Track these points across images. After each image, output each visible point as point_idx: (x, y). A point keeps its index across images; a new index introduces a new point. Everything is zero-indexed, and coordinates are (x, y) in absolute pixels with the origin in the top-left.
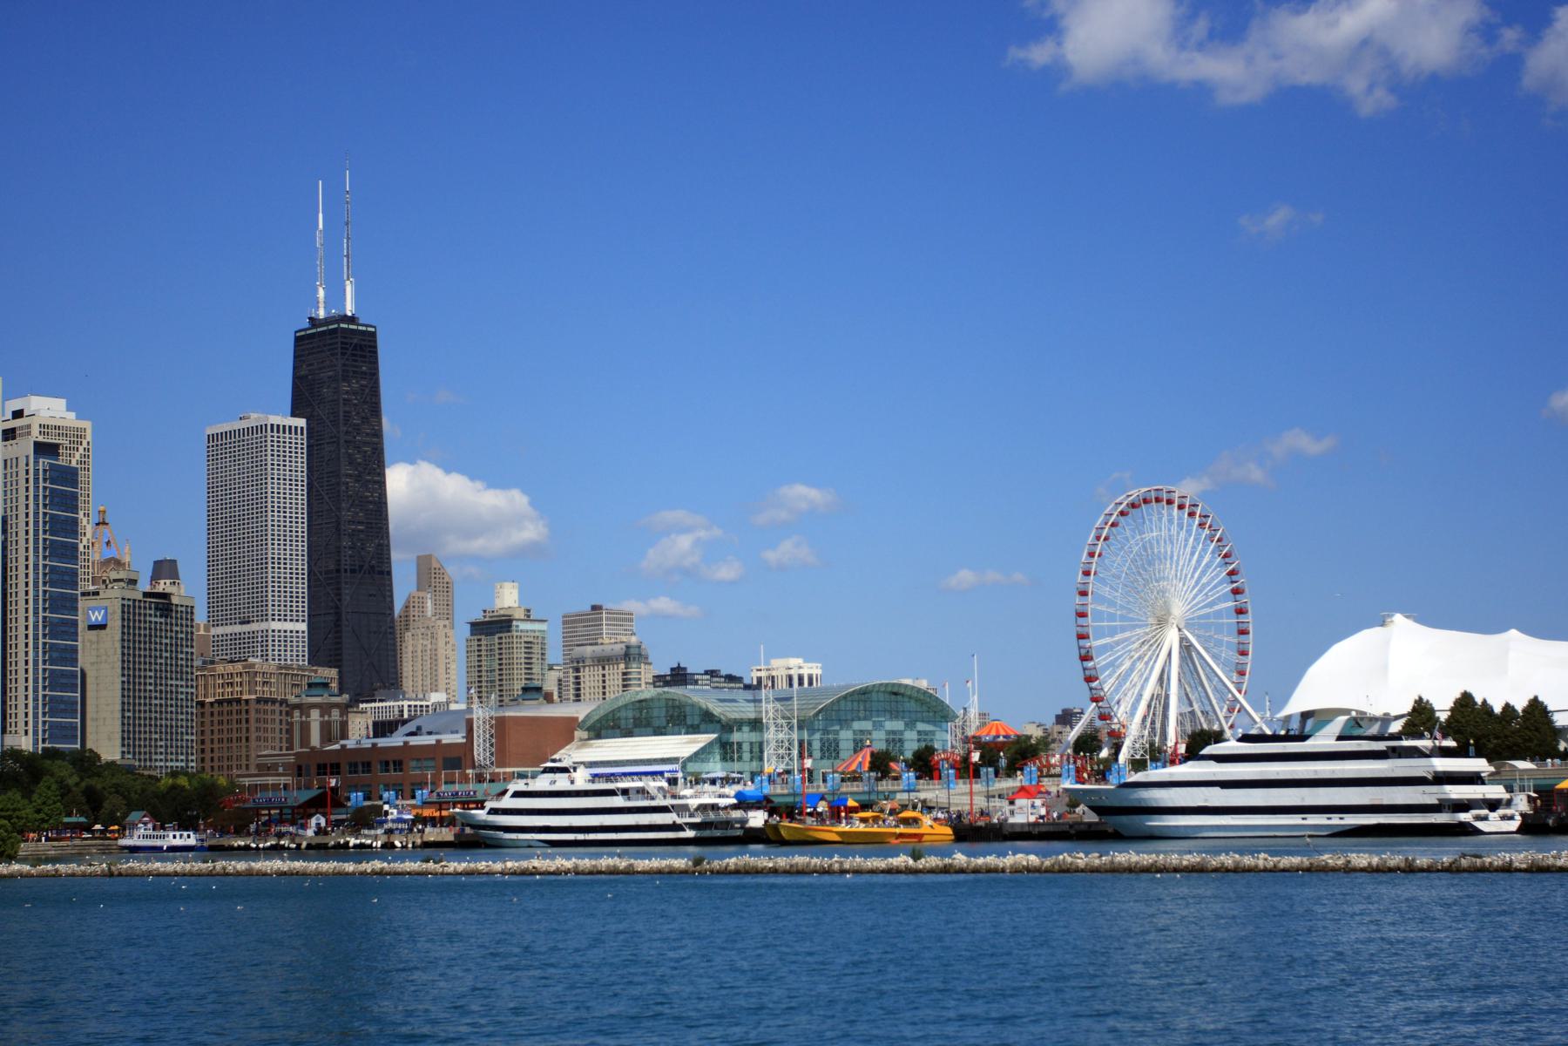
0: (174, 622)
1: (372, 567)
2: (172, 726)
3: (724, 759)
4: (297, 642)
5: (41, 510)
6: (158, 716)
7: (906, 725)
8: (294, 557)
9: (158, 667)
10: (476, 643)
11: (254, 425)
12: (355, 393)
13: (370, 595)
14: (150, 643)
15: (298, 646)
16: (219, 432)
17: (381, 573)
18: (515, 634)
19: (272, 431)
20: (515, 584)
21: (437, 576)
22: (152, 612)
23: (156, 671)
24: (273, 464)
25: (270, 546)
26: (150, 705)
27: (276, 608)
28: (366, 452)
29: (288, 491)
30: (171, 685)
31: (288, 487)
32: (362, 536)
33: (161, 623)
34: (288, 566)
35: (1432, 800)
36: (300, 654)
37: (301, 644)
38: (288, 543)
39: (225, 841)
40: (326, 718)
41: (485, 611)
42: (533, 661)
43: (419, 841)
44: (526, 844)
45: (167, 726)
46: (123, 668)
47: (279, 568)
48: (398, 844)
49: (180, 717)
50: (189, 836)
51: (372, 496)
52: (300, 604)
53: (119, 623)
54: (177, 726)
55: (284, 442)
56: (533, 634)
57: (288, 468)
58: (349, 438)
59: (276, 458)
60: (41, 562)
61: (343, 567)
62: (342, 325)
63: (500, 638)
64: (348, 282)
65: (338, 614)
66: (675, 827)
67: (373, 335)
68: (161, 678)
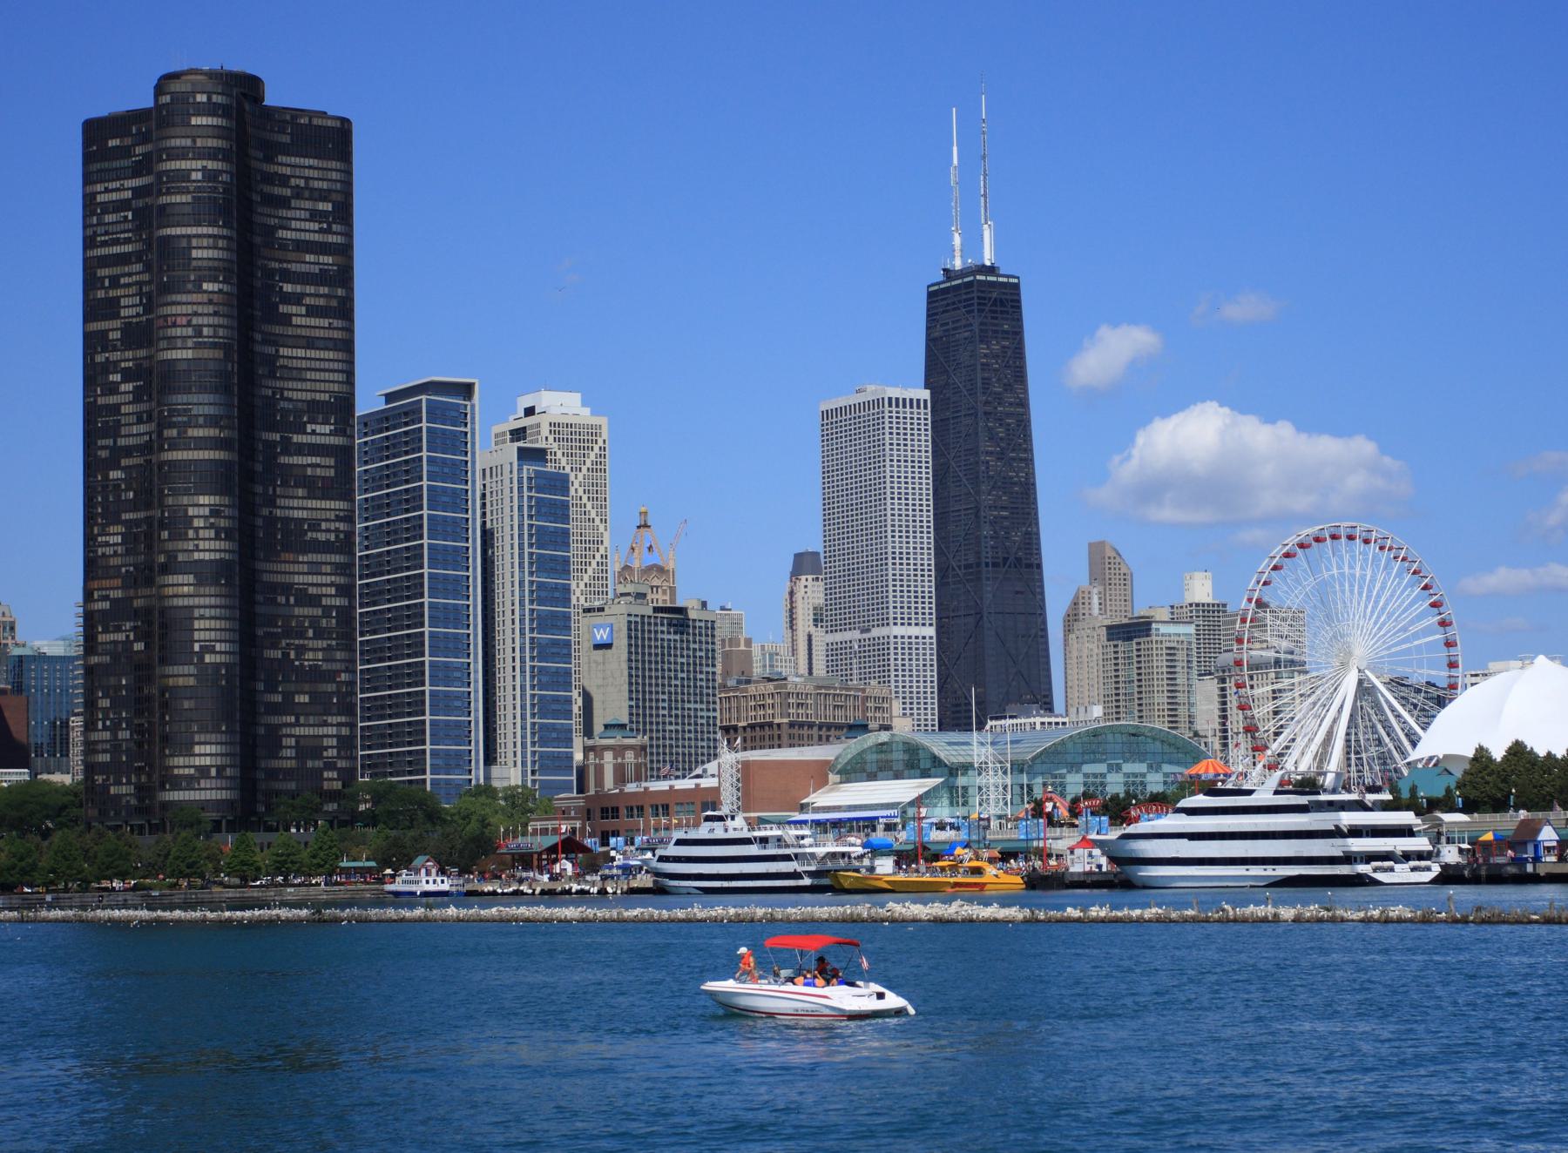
0: (691, 638)
1: (1019, 560)
2: (690, 754)
3: (951, 804)
4: (924, 649)
5: (526, 522)
6: (674, 743)
7: (1150, 767)
8: (919, 551)
9: (673, 689)
10: (1113, 649)
11: (870, 399)
12: (996, 356)
13: (1017, 593)
14: (663, 662)
15: (924, 654)
16: (852, 403)
17: (1029, 566)
18: (1154, 638)
19: (890, 405)
20: (1209, 574)
21: (1112, 566)
22: (665, 629)
23: (670, 693)
24: (891, 444)
25: (890, 539)
26: (664, 731)
27: (899, 610)
28: (1009, 425)
29: (910, 475)
30: (689, 709)
31: (910, 469)
32: (1006, 523)
33: (675, 641)
34: (912, 561)
35: (1338, 853)
36: (928, 663)
37: (928, 652)
38: (911, 534)
39: (476, 885)
40: (619, 760)
41: (1172, 607)
42: (1177, 669)
43: (625, 887)
44: (685, 891)
45: (684, 754)
46: (631, 692)
47: (901, 564)
48: (610, 890)
49: (700, 744)
50: (443, 882)
51: (1017, 476)
52: (927, 605)
53: (625, 642)
54: (697, 754)
55: (905, 418)
56: (1176, 638)
57: (909, 448)
58: (988, 409)
59: (895, 436)
60: (527, 579)
61: (984, 560)
62: (978, 277)
63: (1139, 644)
64: (986, 226)
65: (979, 614)
66: (795, 875)
67: (1016, 287)
68: (676, 701)
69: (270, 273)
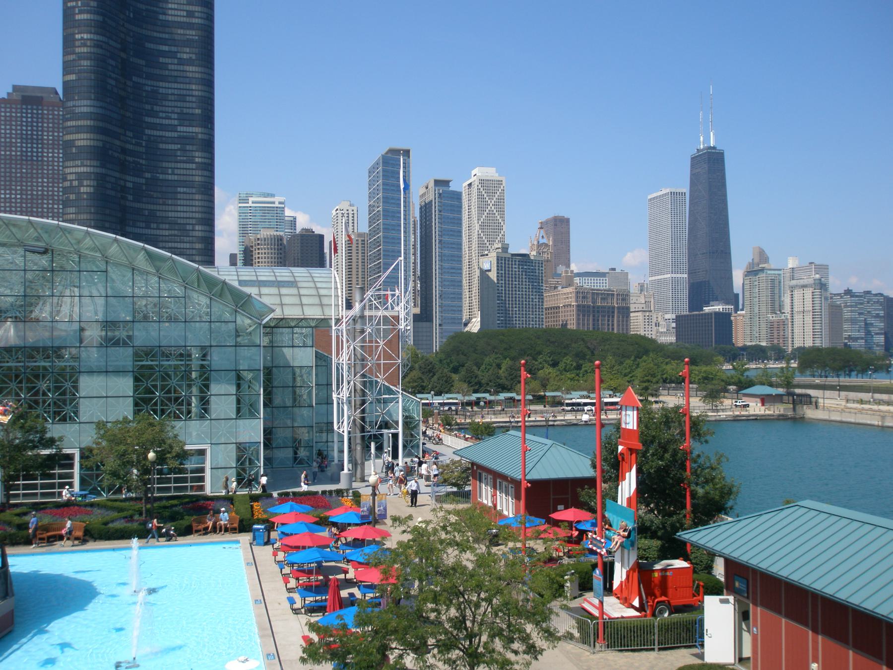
1: (722, 251)
17: (726, 253)
53: (496, 268)
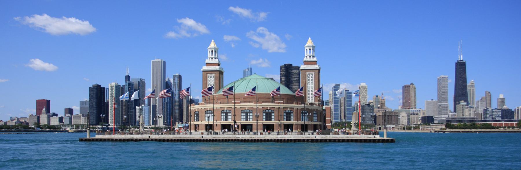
67: (465, 62)
69: (292, 80)
